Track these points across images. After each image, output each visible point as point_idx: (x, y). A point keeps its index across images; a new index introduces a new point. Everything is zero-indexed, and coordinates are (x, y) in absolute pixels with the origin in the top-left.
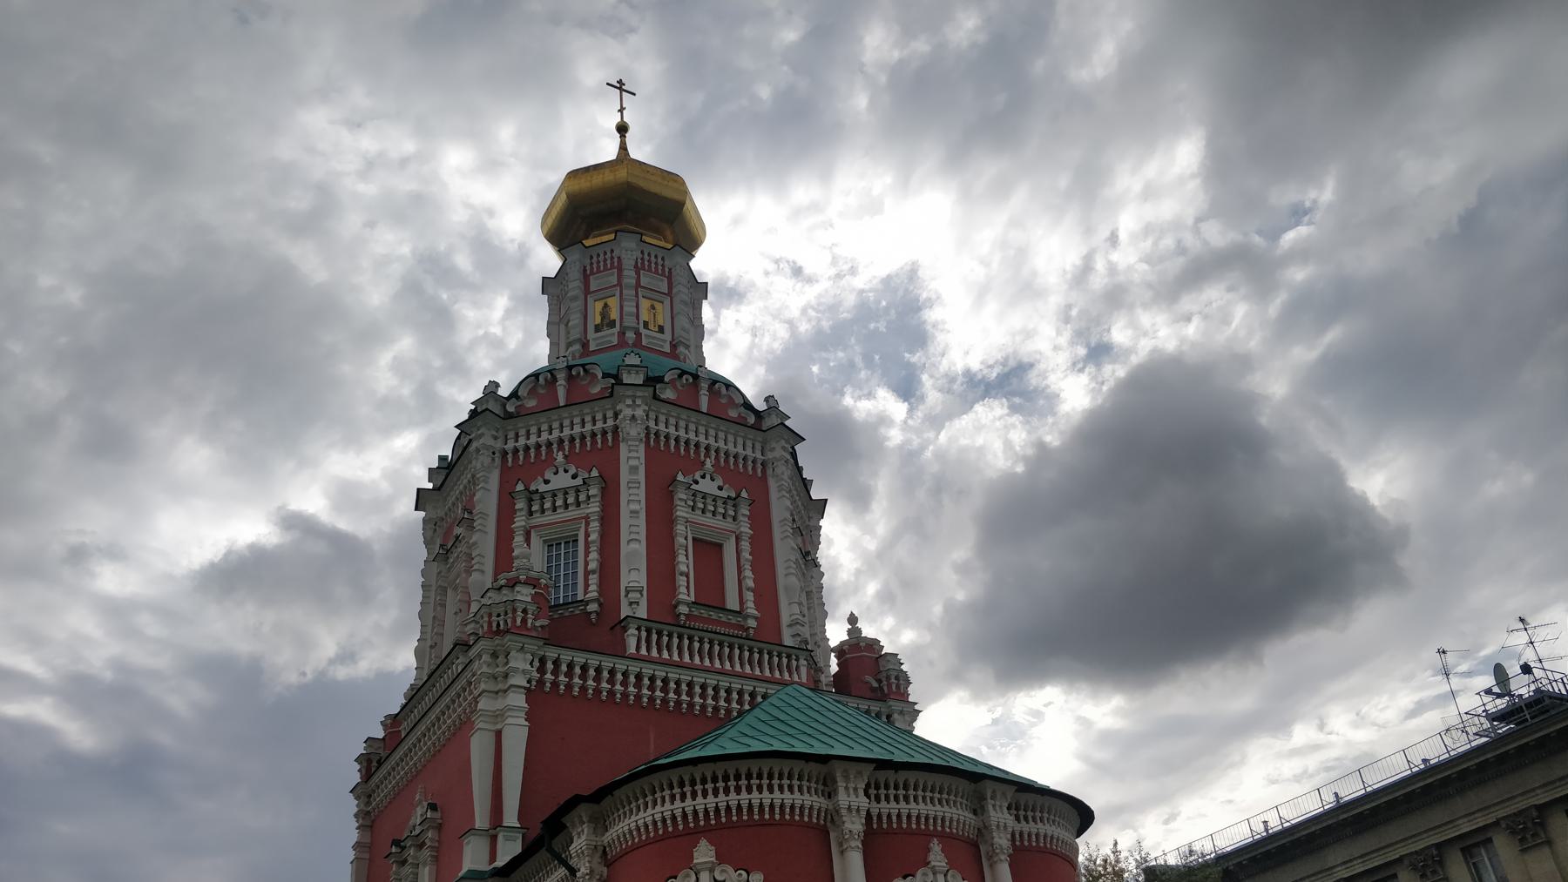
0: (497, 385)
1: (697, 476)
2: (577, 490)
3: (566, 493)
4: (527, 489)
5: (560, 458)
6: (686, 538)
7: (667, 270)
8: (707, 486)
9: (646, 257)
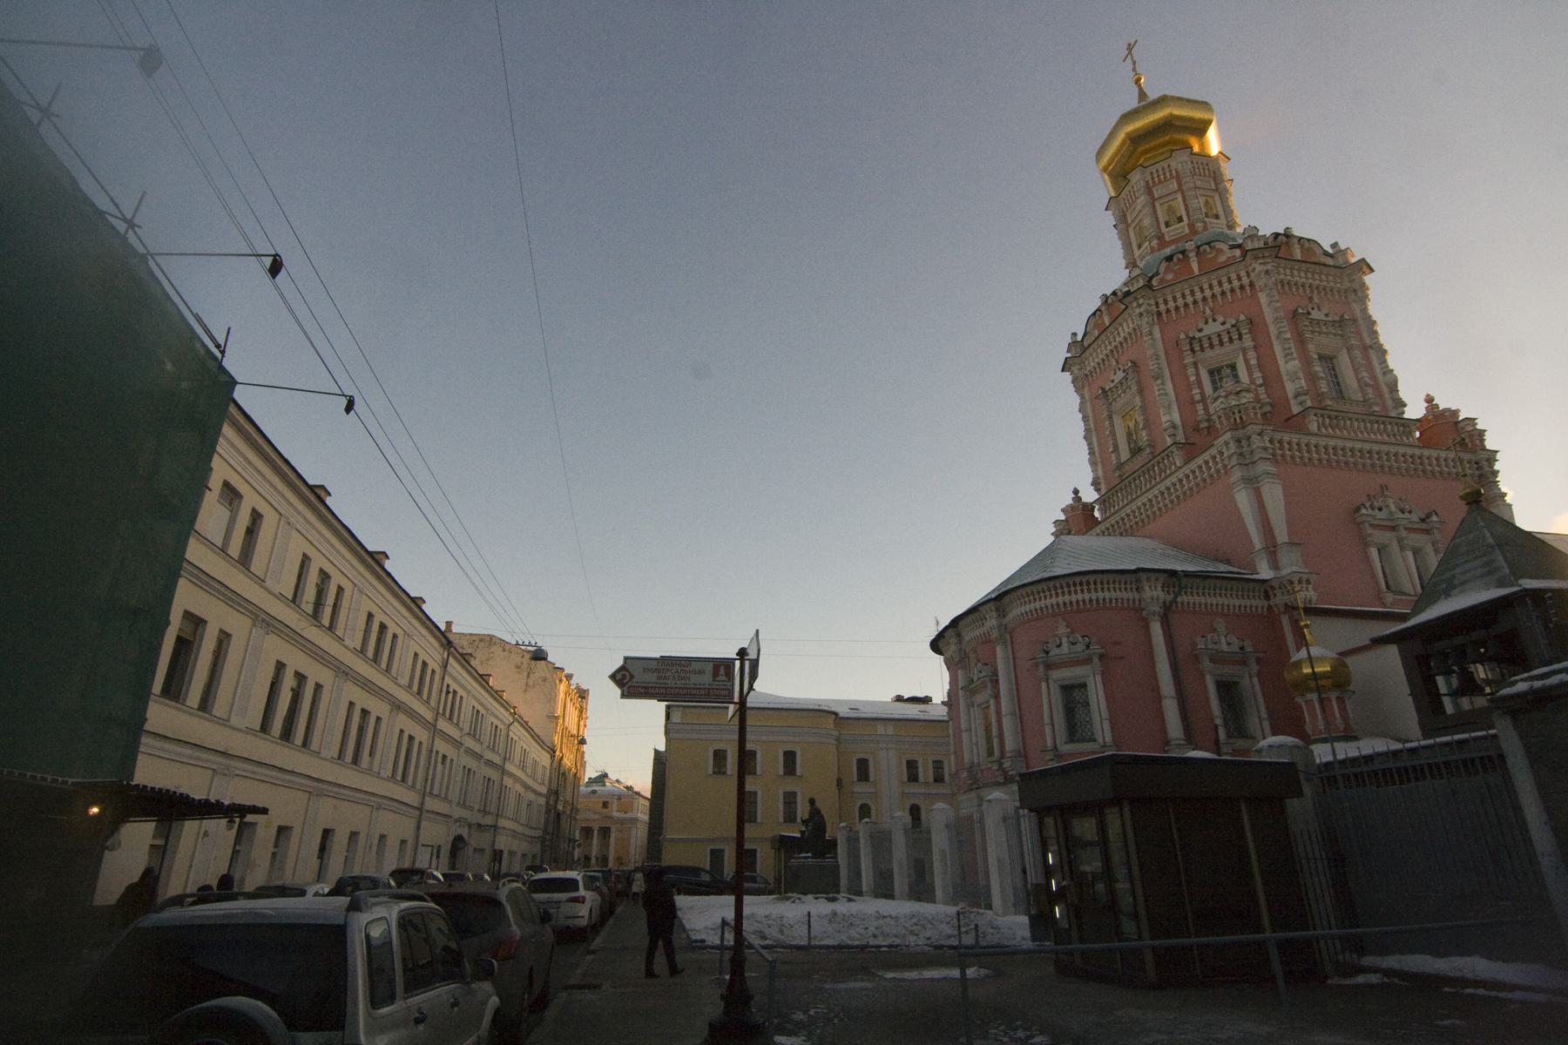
0: (1074, 334)
1: (1201, 326)
2: (1126, 378)
3: (1122, 384)
4: (1103, 389)
5: (1114, 363)
6: (1198, 375)
7: (1174, 172)
8: (1212, 328)
9: (1155, 175)
